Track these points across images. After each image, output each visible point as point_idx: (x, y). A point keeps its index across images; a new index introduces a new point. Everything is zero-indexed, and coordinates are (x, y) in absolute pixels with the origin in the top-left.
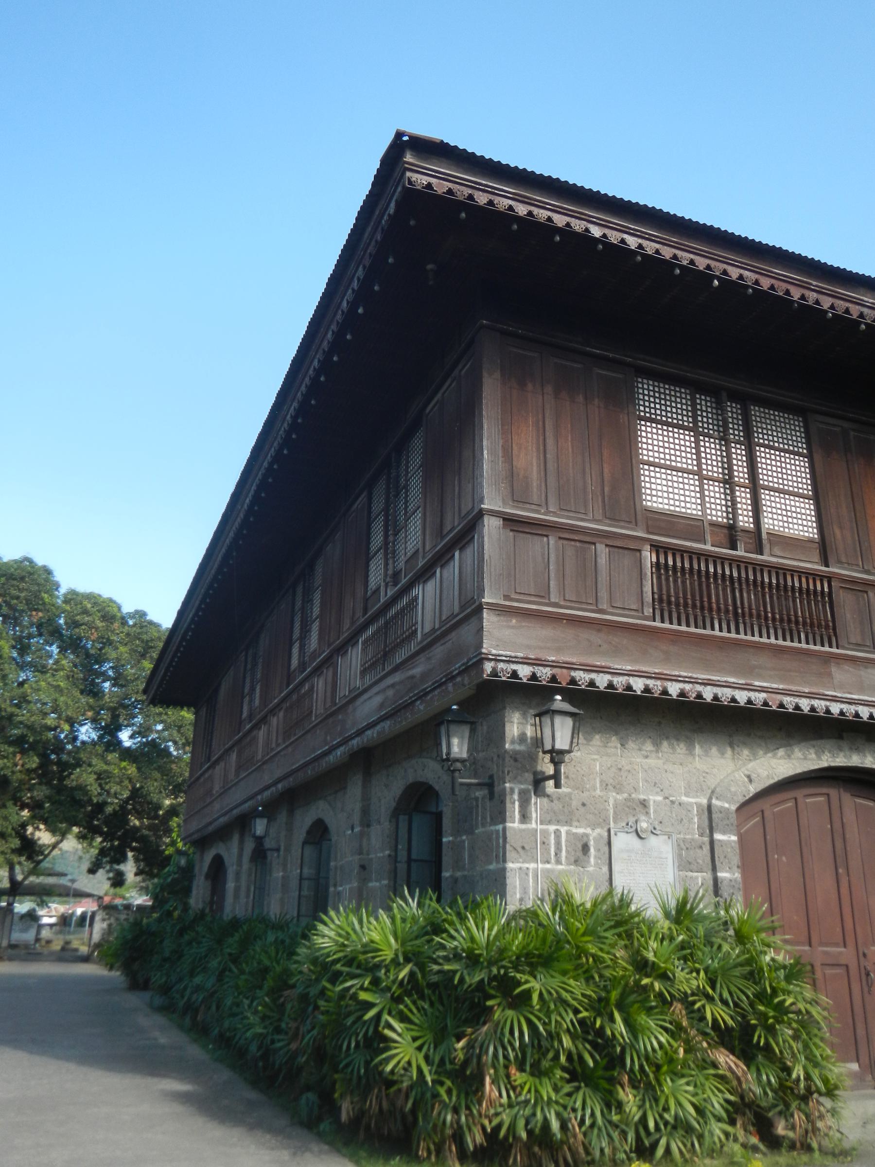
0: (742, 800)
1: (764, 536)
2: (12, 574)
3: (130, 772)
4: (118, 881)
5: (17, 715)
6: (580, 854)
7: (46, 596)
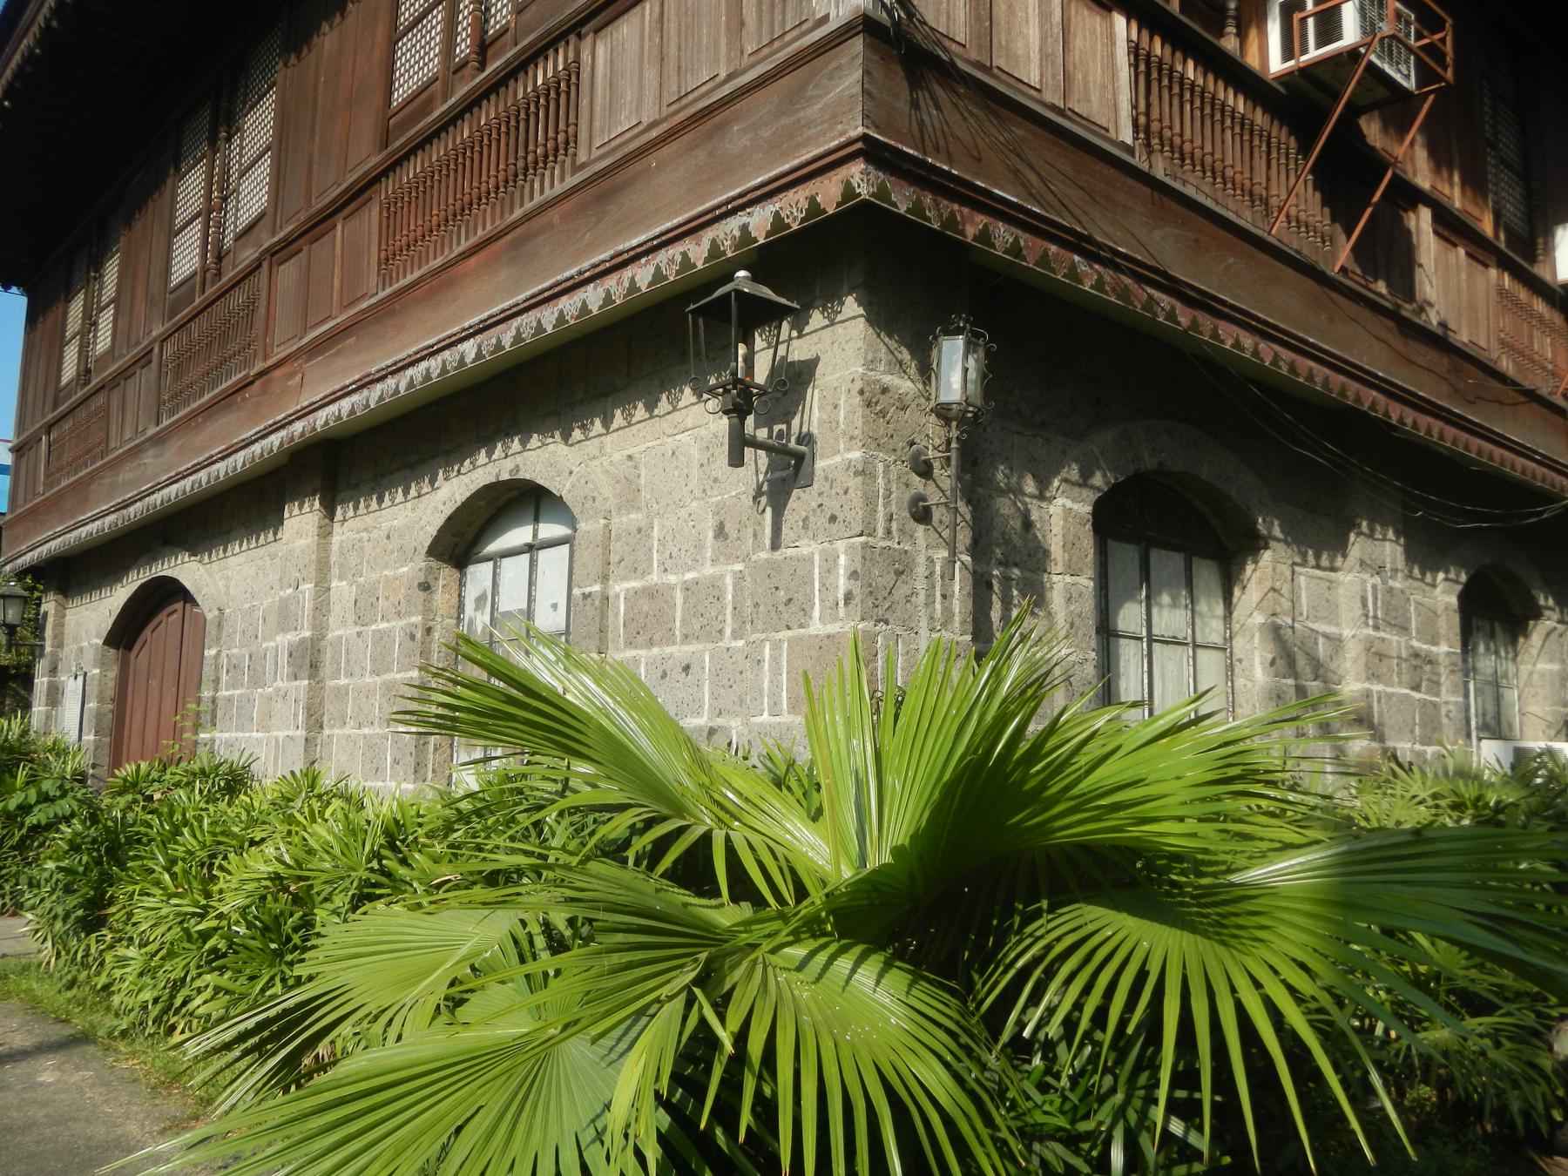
0: (105, 634)
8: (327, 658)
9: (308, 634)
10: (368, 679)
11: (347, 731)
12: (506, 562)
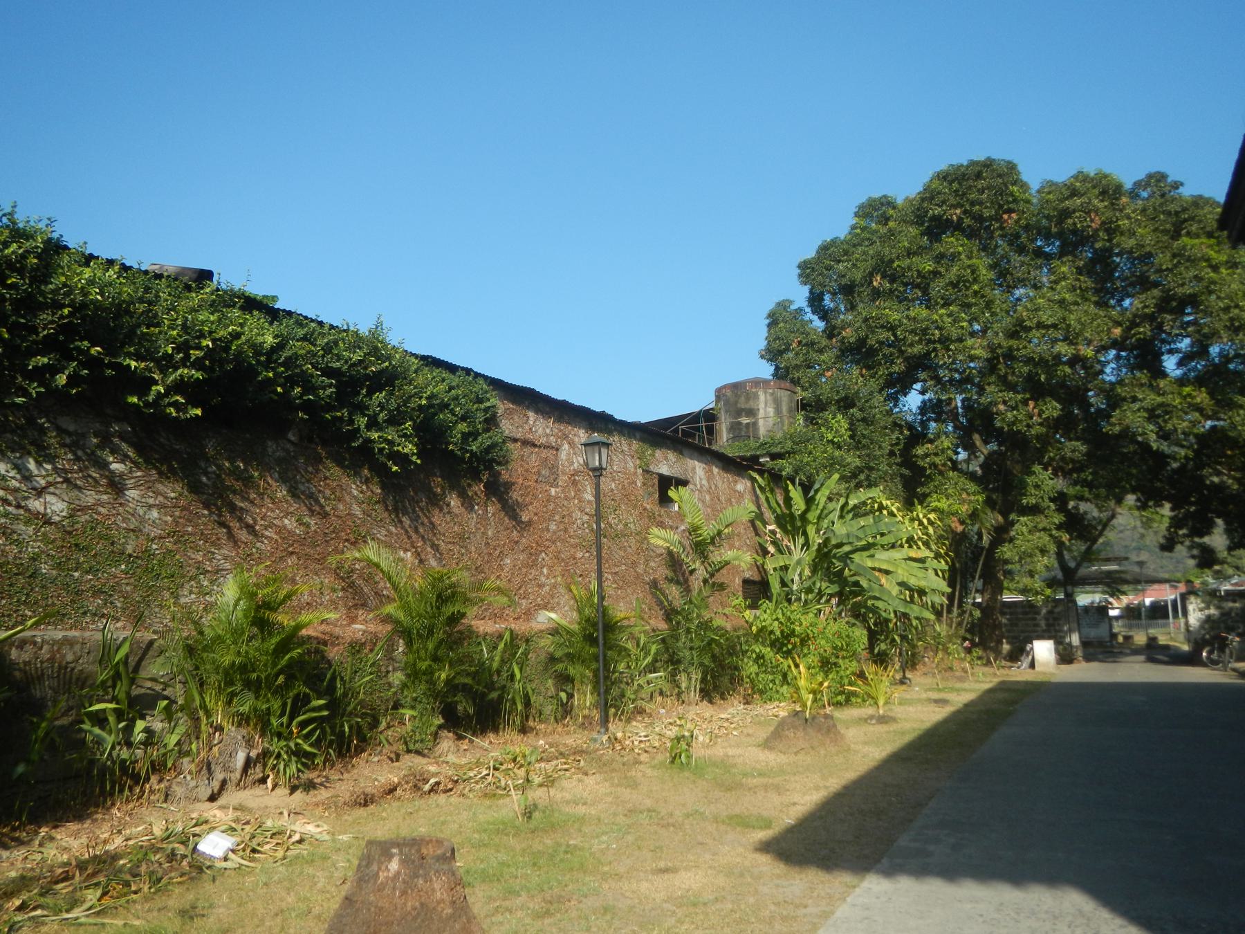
2: (964, 175)
3: (1199, 400)
4: (1207, 559)
5: (1018, 349)
7: (1015, 189)
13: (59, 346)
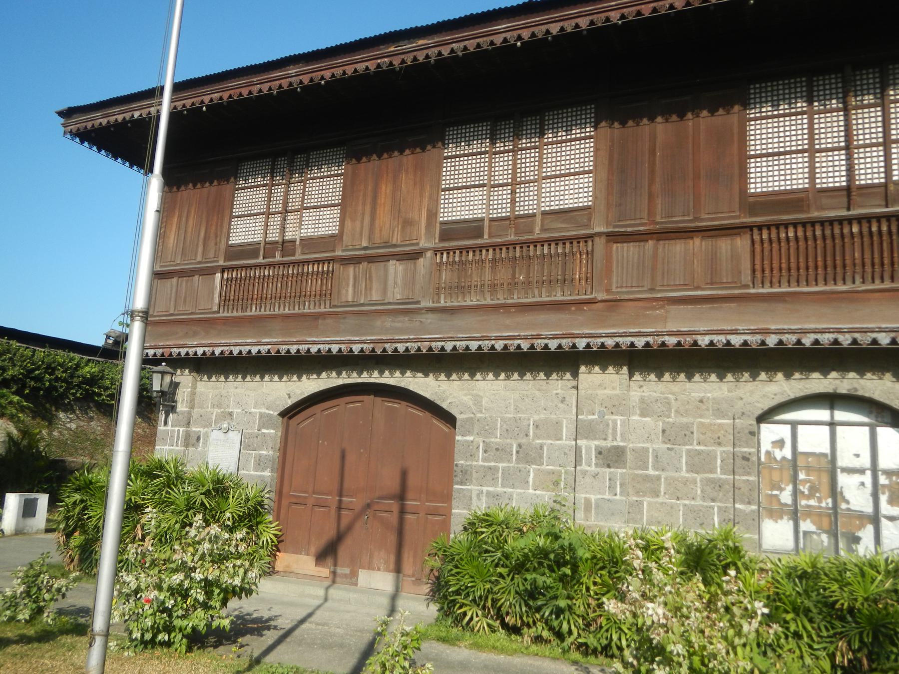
0: (282, 409)
1: (298, 242)
6: (195, 441)
8: (629, 456)
9: (622, 444)
10: (684, 473)
11: (660, 500)
12: (800, 427)
13: (79, 386)
